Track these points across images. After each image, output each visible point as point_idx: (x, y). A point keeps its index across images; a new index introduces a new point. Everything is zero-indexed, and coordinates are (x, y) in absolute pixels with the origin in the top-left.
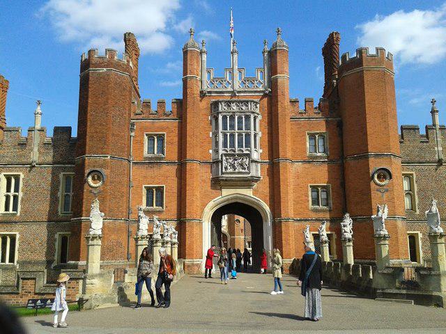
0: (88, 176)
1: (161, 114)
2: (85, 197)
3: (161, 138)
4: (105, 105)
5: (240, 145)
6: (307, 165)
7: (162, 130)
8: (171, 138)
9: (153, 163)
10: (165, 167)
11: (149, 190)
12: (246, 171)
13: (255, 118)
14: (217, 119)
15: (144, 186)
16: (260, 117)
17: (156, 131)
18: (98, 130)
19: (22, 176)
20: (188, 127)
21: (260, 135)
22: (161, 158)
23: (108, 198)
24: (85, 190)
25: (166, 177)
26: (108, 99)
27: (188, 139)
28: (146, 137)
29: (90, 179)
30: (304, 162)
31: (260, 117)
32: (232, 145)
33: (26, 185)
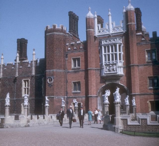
0: (48, 78)
1: (78, 49)
2: (47, 87)
3: (78, 59)
4: (53, 48)
5: (113, 60)
6: (147, 67)
7: (79, 56)
8: (82, 59)
9: (76, 71)
10: (81, 72)
11: (75, 83)
12: (116, 72)
13: (120, 46)
14: (101, 48)
15: (72, 82)
16: (122, 45)
17: (76, 57)
18: (50, 59)
19: (29, 80)
20: (88, 53)
21: (122, 53)
22: (79, 69)
23: (55, 88)
24: (47, 85)
25: (80, 78)
26: (53, 46)
27: (89, 59)
28: (72, 60)
29: (48, 80)
30: (145, 65)
31: (122, 45)
32: (109, 60)
33: (30, 84)
